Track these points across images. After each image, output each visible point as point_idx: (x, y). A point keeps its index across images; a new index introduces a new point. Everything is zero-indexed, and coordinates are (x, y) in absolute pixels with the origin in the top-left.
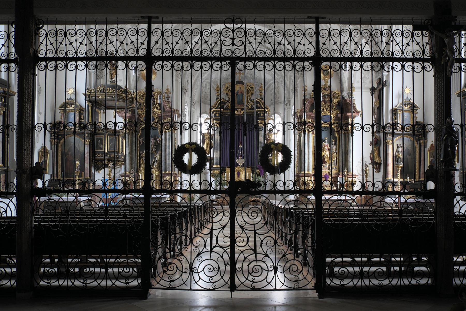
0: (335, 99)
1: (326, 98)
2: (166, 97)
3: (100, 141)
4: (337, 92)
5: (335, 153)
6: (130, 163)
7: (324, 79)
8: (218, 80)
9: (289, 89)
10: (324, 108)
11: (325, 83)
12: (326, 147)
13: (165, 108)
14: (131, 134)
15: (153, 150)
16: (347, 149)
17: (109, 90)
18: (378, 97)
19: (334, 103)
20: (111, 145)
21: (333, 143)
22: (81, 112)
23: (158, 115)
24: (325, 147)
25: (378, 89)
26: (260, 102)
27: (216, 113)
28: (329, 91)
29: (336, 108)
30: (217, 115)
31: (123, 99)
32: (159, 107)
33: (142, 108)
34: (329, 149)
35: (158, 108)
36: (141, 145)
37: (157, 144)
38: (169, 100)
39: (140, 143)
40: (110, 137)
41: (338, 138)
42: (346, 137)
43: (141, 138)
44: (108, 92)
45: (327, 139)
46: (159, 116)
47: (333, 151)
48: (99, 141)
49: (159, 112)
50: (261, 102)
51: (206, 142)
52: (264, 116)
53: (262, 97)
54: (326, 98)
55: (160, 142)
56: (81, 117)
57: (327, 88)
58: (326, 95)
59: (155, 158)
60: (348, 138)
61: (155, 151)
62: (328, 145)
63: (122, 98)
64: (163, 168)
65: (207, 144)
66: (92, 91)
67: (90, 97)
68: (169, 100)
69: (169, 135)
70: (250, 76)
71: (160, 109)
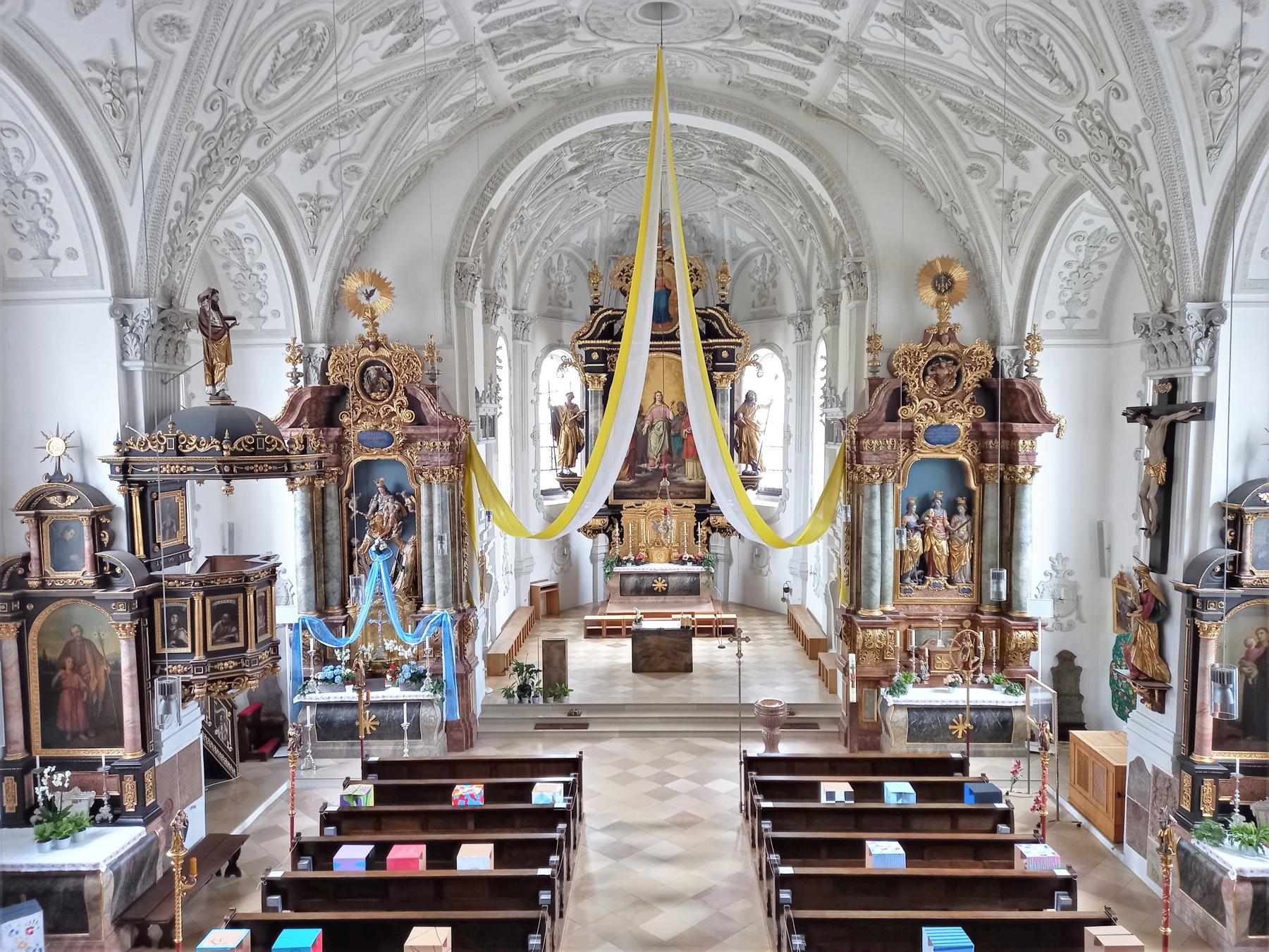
0: (971, 369)
1: (940, 367)
3: (179, 619)
4: (979, 349)
5: (967, 541)
6: (320, 581)
7: (937, 307)
8: (595, 244)
9: (809, 279)
10: (936, 402)
11: (940, 317)
12: (939, 523)
16: (1007, 533)
17: (198, 443)
18: (1164, 448)
19: (969, 385)
20: (218, 627)
21: (962, 509)
22: (99, 522)
24: (934, 521)
25: (1166, 419)
26: (721, 318)
27: (593, 351)
28: (952, 346)
29: (972, 399)
30: (595, 356)
31: (252, 471)
32: (405, 399)
34: (946, 530)
38: (436, 383)
39: (350, 511)
40: (212, 602)
41: (977, 496)
42: (1007, 494)
44: (194, 452)
45: (940, 496)
47: (961, 538)
48: (175, 619)
49: (406, 416)
50: (723, 316)
51: (563, 434)
52: (732, 357)
53: (727, 302)
54: (940, 367)
55: (413, 508)
56: (100, 537)
57: (947, 337)
58: (947, 358)
59: (400, 558)
60: (1013, 500)
61: (400, 536)
62: (945, 515)
63: (247, 468)
64: (426, 593)
65: (567, 437)
66: (136, 448)
67: (129, 471)
68: (436, 383)
70: (691, 233)
71: (408, 408)
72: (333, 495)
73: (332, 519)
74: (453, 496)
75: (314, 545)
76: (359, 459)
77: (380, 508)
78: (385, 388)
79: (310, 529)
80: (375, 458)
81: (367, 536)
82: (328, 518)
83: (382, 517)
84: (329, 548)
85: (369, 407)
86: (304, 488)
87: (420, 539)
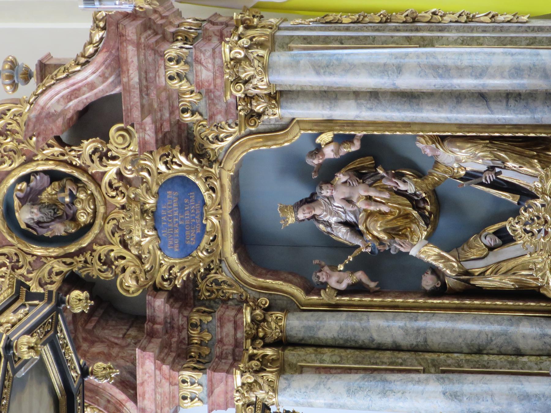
2: (14, 86)
6: (512, 363)
13: (88, 97)
14: (291, 355)
15: (410, 188)
23: (143, 146)
32: (88, 146)
33: (98, 265)
35: (96, 150)
36: (372, 285)
37: (368, 161)
43: (323, 278)
46: (153, 147)
55: (350, 139)
61: (420, 174)
69: (295, 66)
71: (106, 139)
72: (311, 323)
73: (365, 329)
74: (305, 39)
75: (424, 371)
76: (233, 258)
77: (351, 218)
78: (63, 189)
79: (378, 376)
80: (230, 223)
81: (413, 252)
82: (363, 337)
83: (370, 214)
84: (435, 341)
85: (109, 227)
86: (282, 383)
87: (424, 125)
